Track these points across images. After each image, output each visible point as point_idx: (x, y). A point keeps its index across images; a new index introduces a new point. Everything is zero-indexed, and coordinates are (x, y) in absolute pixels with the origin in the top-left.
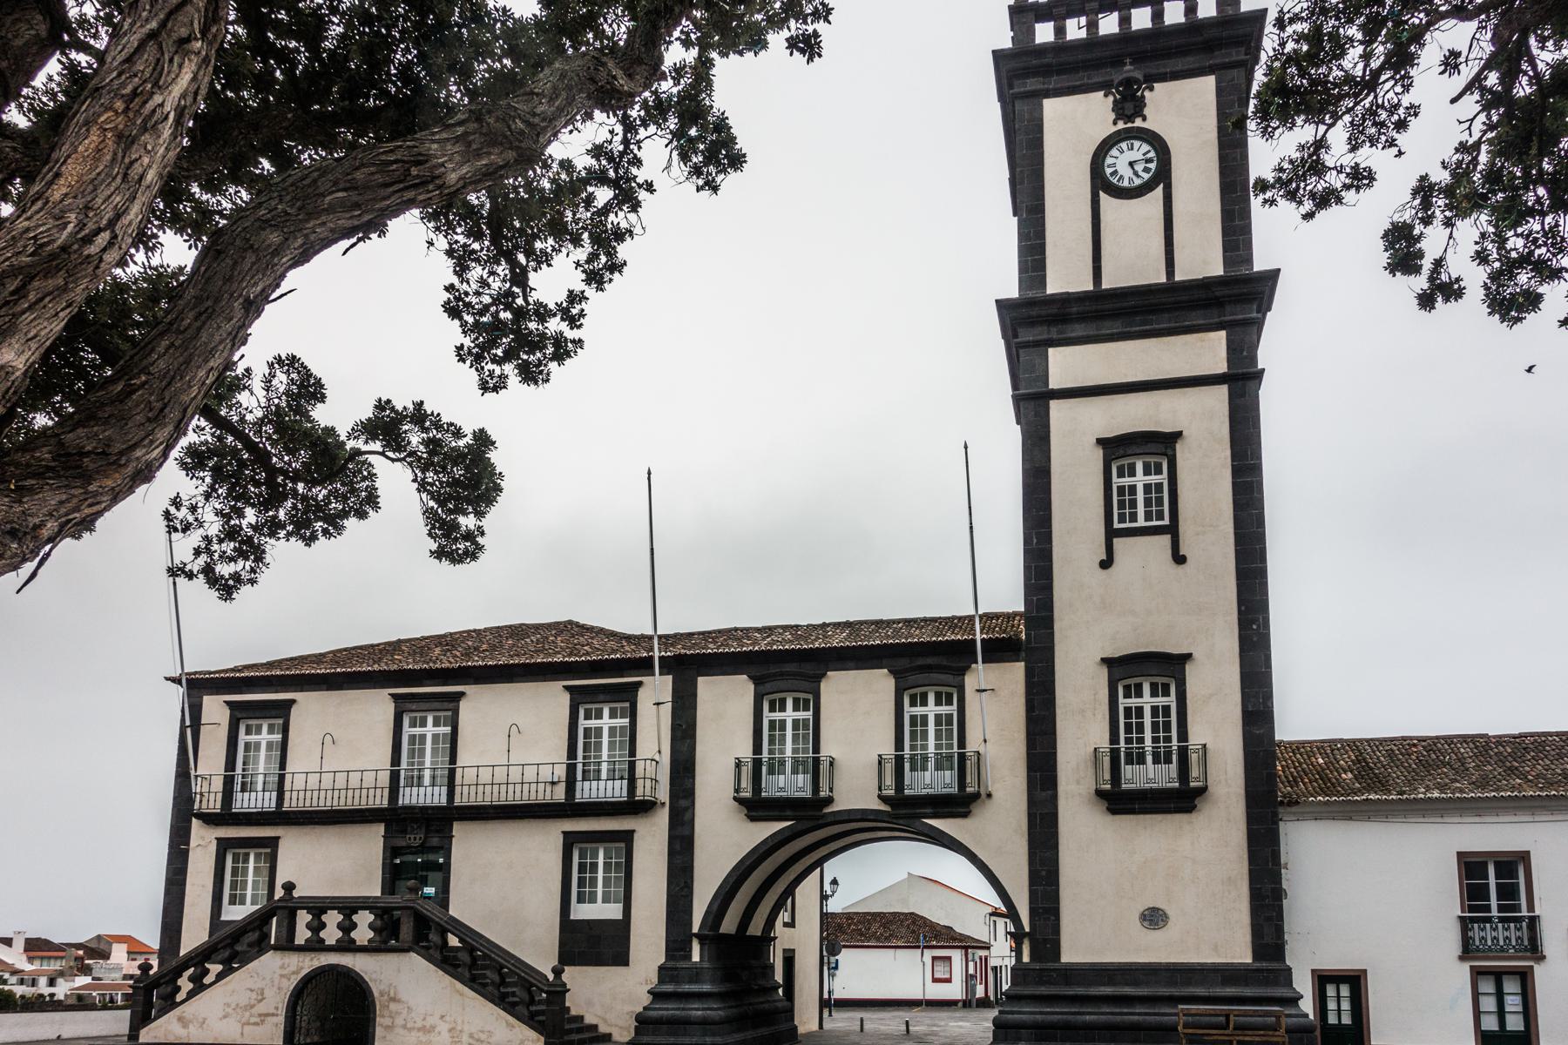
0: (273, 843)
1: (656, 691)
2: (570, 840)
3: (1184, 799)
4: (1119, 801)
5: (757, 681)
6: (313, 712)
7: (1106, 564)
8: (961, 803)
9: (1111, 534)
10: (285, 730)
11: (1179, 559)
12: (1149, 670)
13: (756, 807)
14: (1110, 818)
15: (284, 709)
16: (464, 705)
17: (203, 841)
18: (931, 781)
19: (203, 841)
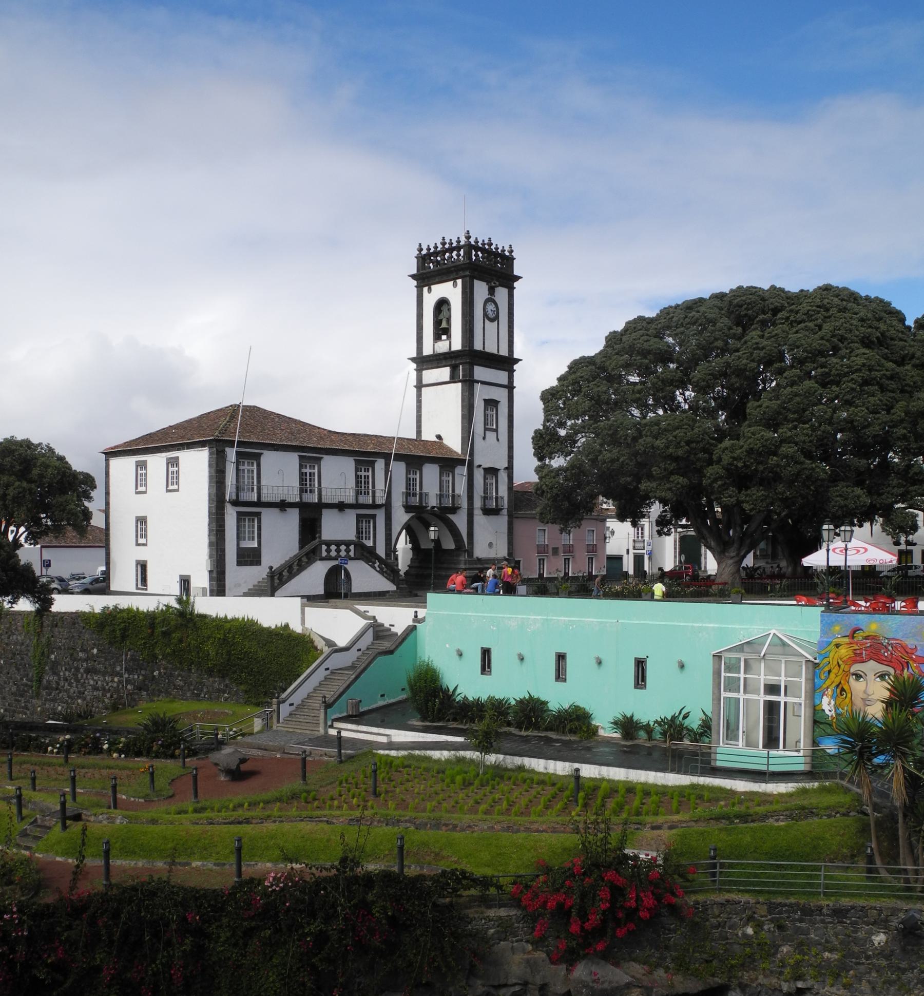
0: (258, 515)
1: (380, 464)
2: (358, 516)
3: (496, 512)
4: (487, 511)
5: (407, 465)
6: (269, 459)
7: (484, 438)
8: (454, 509)
9: (486, 429)
10: (259, 466)
11: (498, 440)
12: (492, 472)
13: (408, 508)
14: (484, 517)
15: (257, 457)
16: (323, 463)
17: (231, 516)
18: (449, 503)
19: (231, 516)
